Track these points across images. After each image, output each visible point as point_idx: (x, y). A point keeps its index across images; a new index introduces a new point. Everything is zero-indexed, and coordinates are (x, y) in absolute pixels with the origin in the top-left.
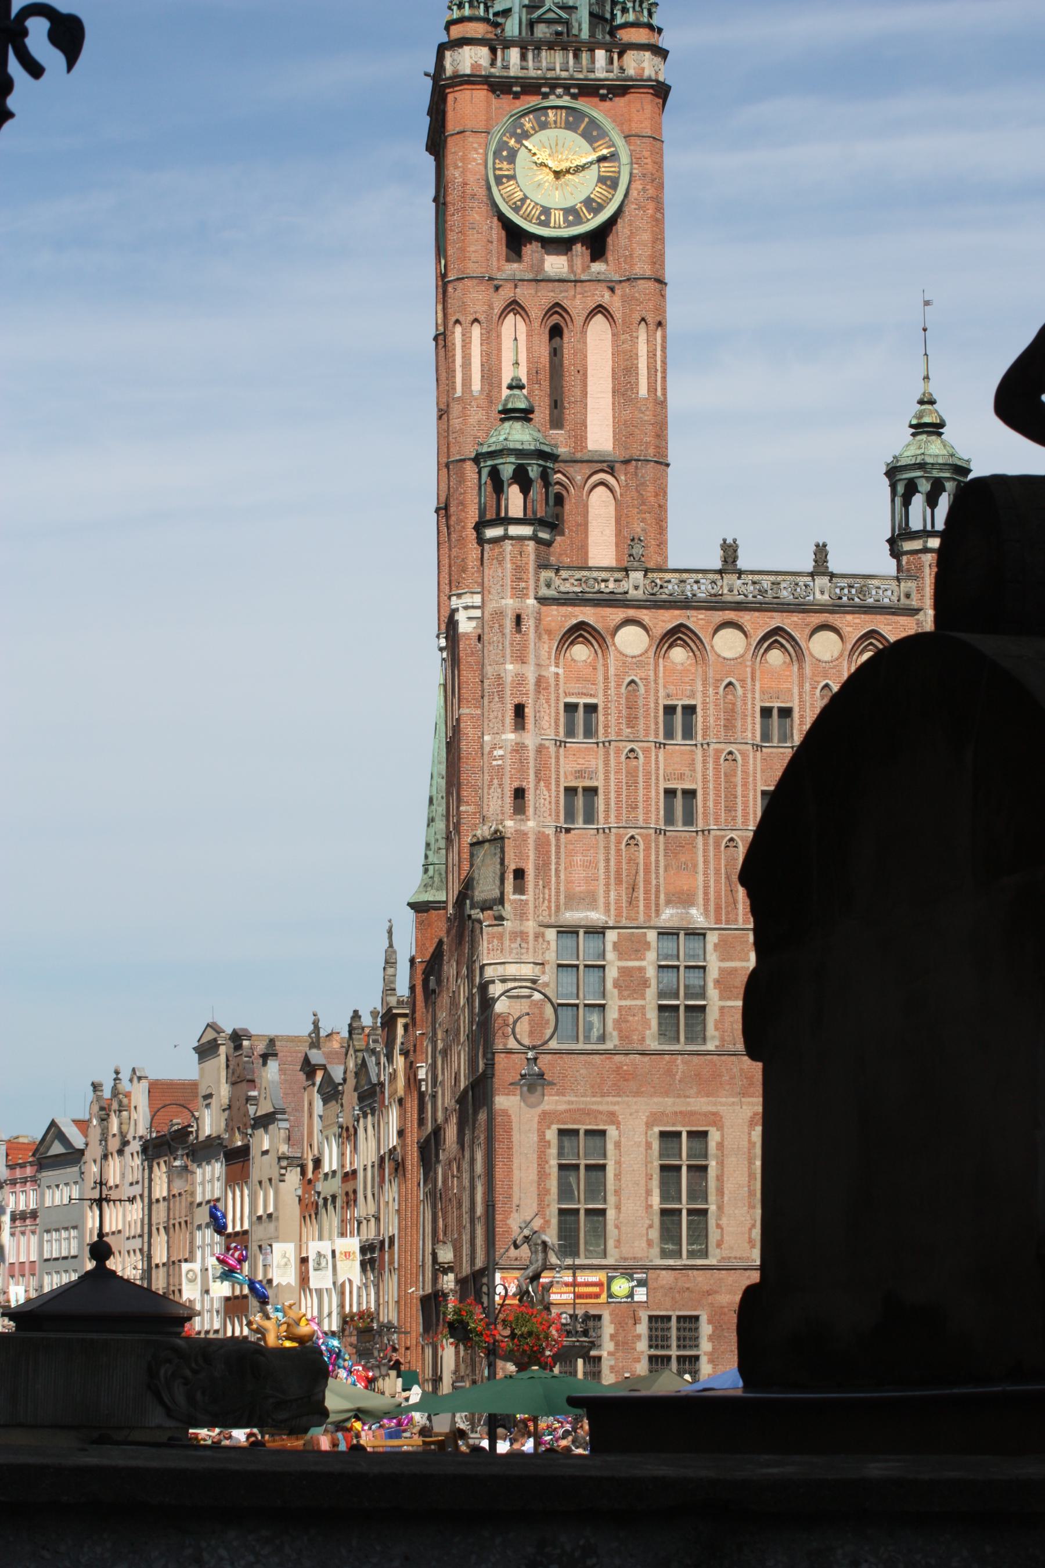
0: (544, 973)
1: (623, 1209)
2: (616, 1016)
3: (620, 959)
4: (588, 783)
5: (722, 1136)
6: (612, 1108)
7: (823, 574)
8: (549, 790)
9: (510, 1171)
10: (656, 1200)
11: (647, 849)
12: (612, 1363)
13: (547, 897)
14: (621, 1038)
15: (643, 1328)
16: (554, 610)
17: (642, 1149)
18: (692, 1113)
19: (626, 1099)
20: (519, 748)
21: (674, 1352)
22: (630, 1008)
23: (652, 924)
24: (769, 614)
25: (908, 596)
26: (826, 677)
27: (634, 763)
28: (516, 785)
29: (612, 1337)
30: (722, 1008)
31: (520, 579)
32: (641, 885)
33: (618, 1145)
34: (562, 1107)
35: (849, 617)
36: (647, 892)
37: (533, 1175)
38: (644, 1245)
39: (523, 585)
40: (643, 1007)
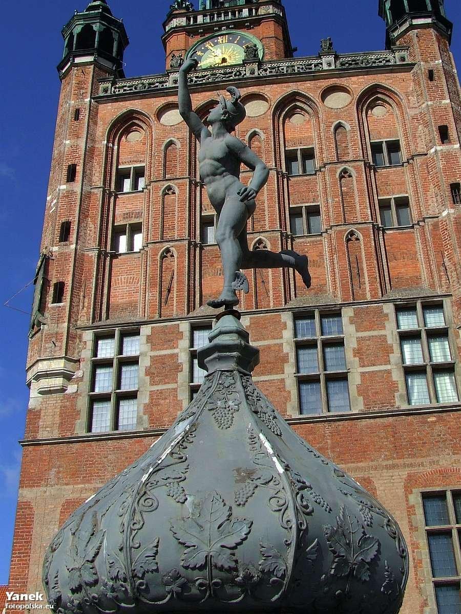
0: (79, 369)
2: (147, 401)
4: (135, 221)
7: (328, 54)
8: (95, 224)
13: (86, 304)
14: (151, 421)
16: (109, 106)
22: (161, 392)
23: (185, 315)
24: (286, 85)
25: (403, 59)
26: (338, 118)
27: (172, 197)
28: (64, 220)
31: (82, 88)
35: (354, 79)
36: (179, 291)
39: (84, 91)
40: (175, 390)
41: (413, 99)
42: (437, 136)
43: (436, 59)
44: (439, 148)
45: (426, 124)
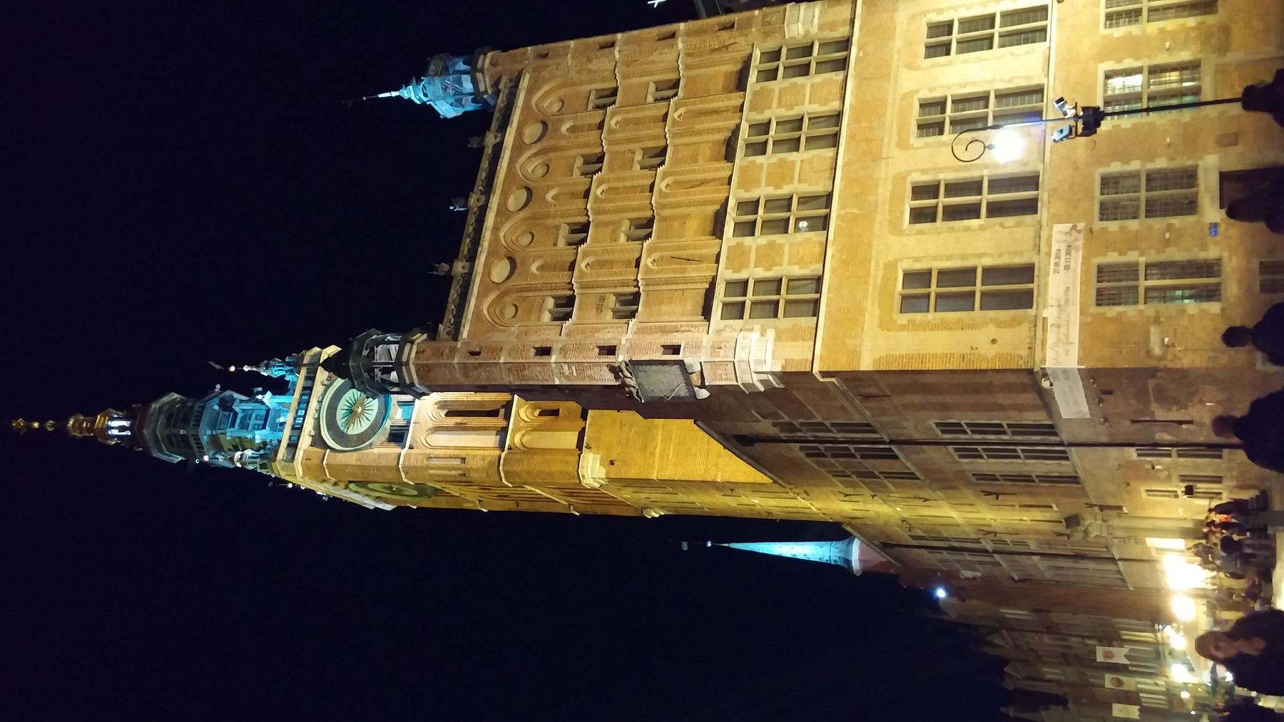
1: (982, 251)
2: (797, 267)
3: (748, 267)
5: (916, 171)
6: (881, 266)
9: (935, 356)
10: (974, 223)
11: (660, 249)
12: (1153, 252)
15: (1113, 226)
17: (923, 237)
18: (892, 196)
19: (874, 253)
20: (563, 350)
21: (1143, 194)
22: (791, 256)
29: (1121, 254)
30: (800, 181)
32: (689, 252)
33: (916, 260)
34: (877, 311)
37: (945, 333)
38: (1020, 230)
40: (792, 245)
41: (559, 73)
42: (606, 50)
43: (525, 53)
44: (617, 48)
45: (589, 60)
